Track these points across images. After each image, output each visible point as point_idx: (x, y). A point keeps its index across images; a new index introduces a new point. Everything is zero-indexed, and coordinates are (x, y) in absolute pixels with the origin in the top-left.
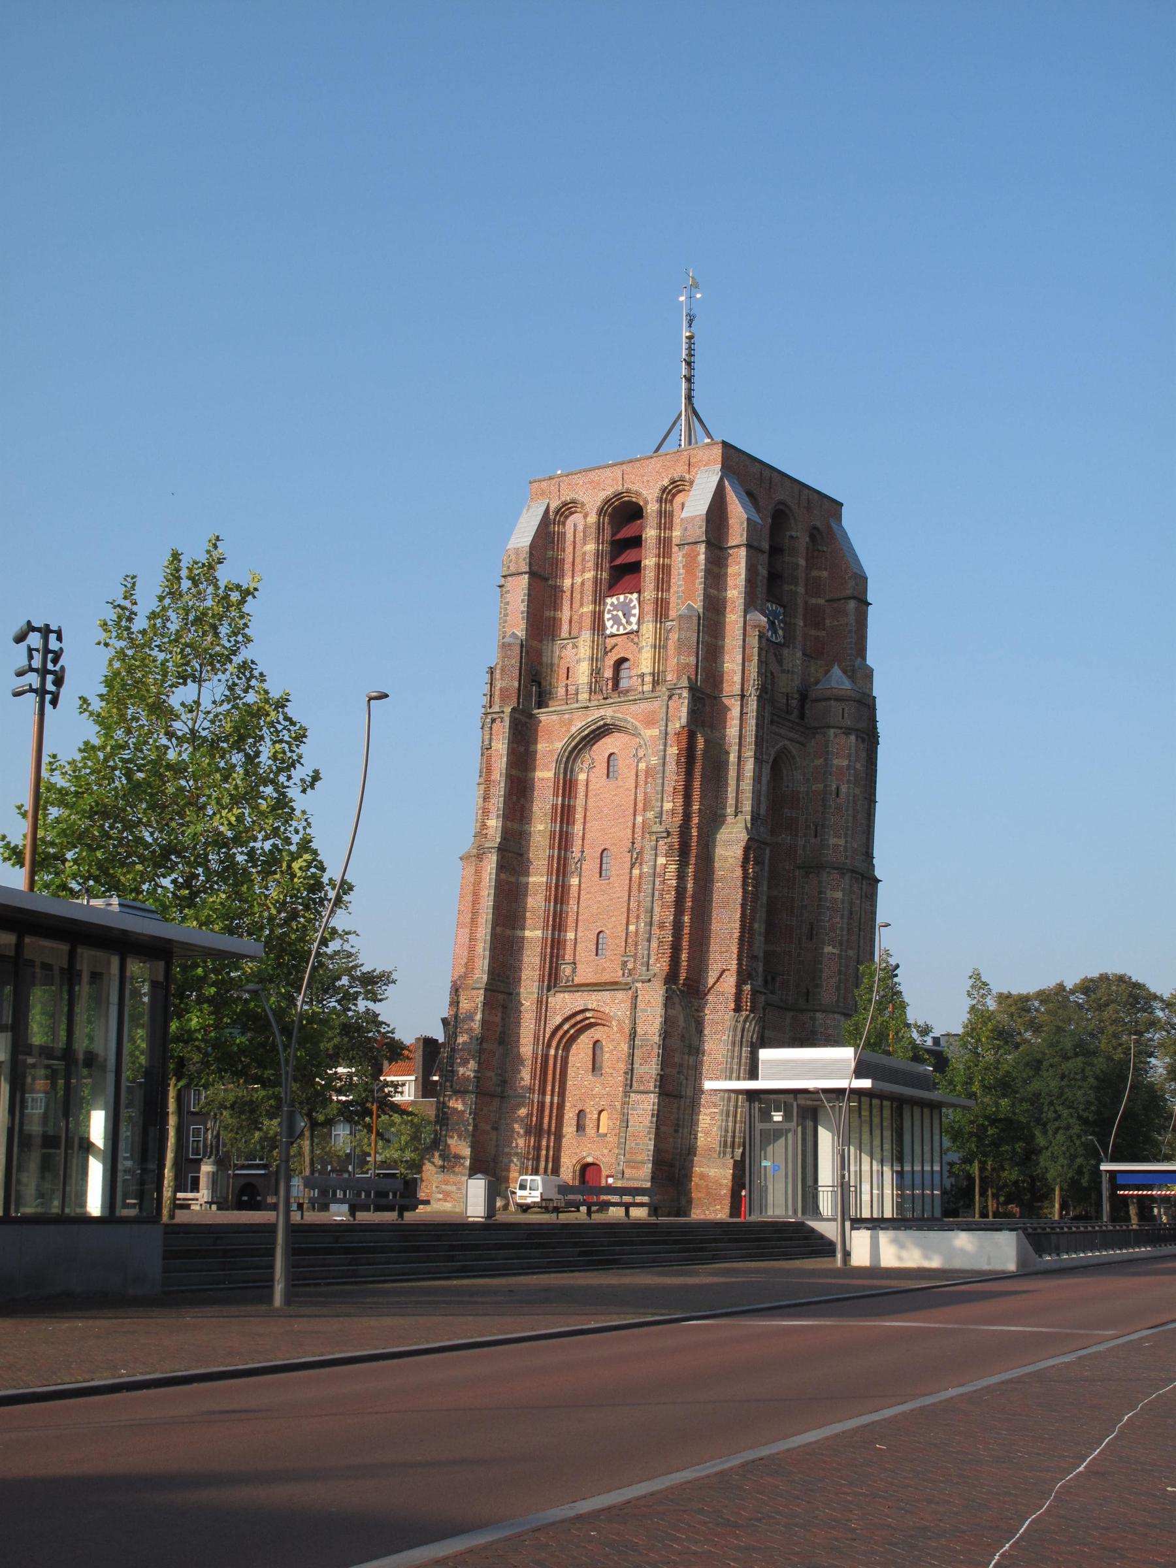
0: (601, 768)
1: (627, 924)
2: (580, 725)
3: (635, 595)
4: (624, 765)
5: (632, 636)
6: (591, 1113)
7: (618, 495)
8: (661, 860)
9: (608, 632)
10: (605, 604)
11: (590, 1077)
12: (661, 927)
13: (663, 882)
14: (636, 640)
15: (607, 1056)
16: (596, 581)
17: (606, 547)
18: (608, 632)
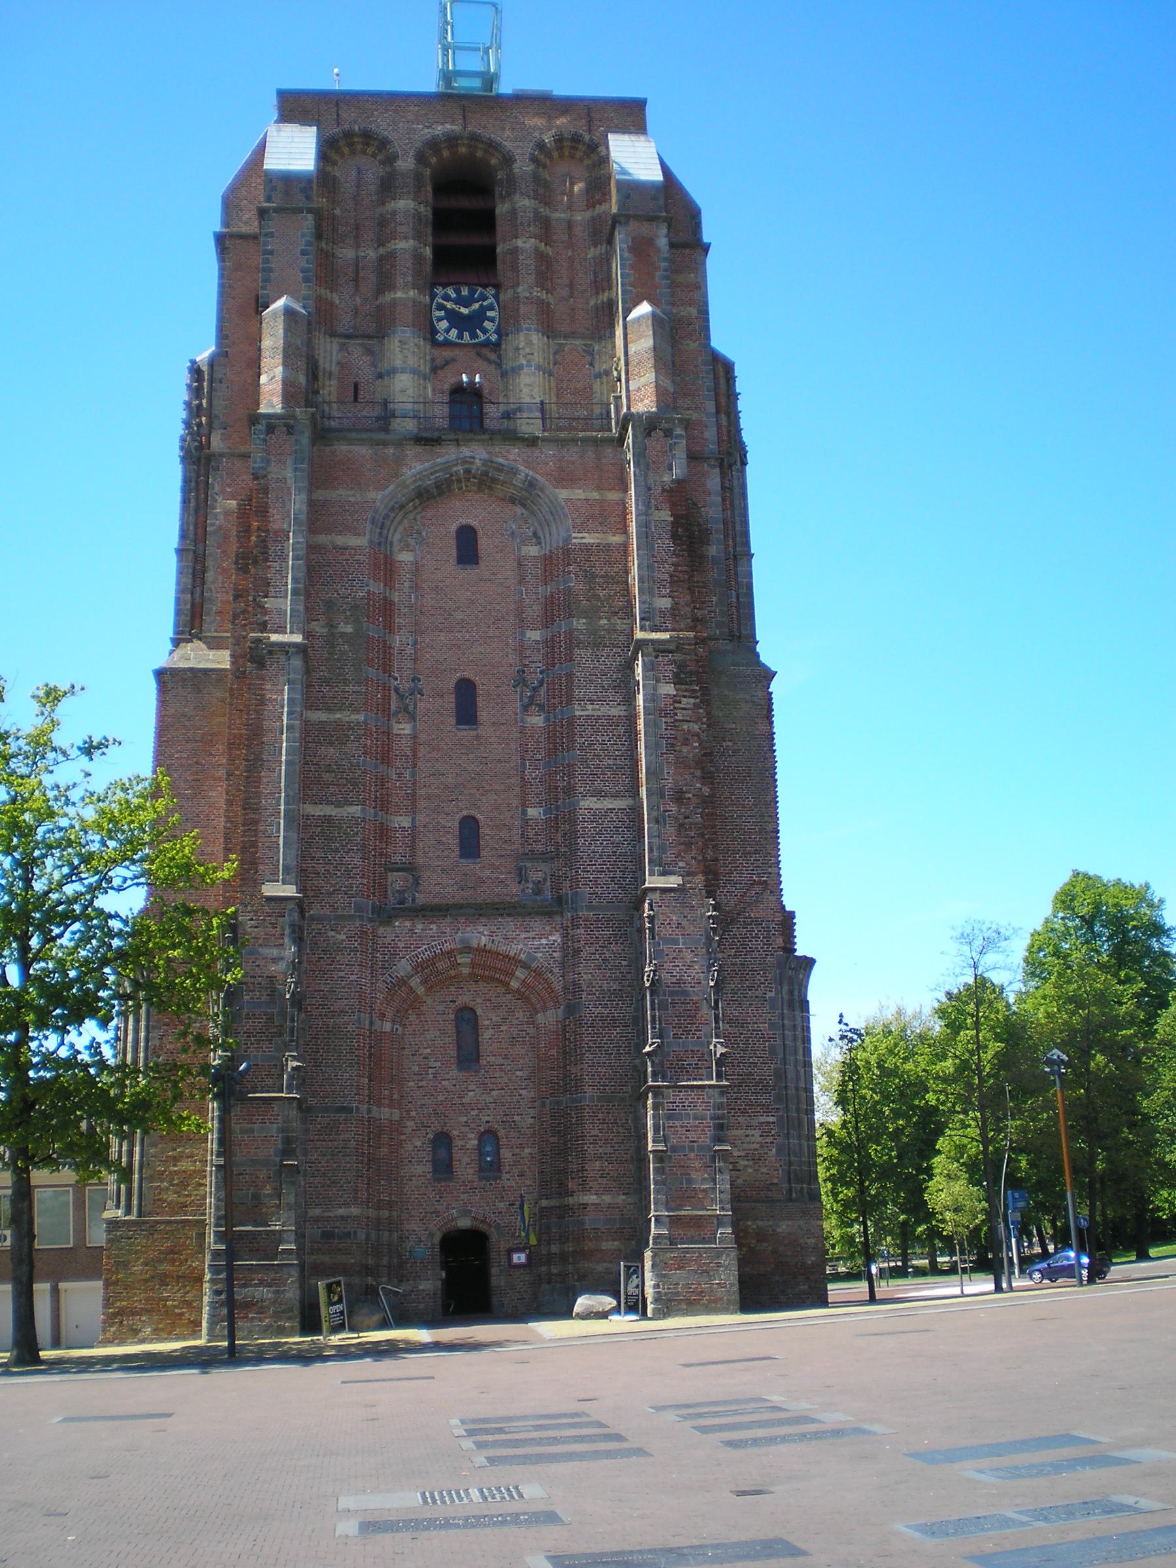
2: (419, 467)
3: (490, 291)
5: (485, 351)
6: (463, 1136)
7: (452, 140)
8: (670, 689)
9: (440, 337)
10: (433, 296)
11: (455, 1073)
13: (674, 725)
14: (493, 357)
15: (486, 1035)
16: (418, 258)
17: (426, 211)
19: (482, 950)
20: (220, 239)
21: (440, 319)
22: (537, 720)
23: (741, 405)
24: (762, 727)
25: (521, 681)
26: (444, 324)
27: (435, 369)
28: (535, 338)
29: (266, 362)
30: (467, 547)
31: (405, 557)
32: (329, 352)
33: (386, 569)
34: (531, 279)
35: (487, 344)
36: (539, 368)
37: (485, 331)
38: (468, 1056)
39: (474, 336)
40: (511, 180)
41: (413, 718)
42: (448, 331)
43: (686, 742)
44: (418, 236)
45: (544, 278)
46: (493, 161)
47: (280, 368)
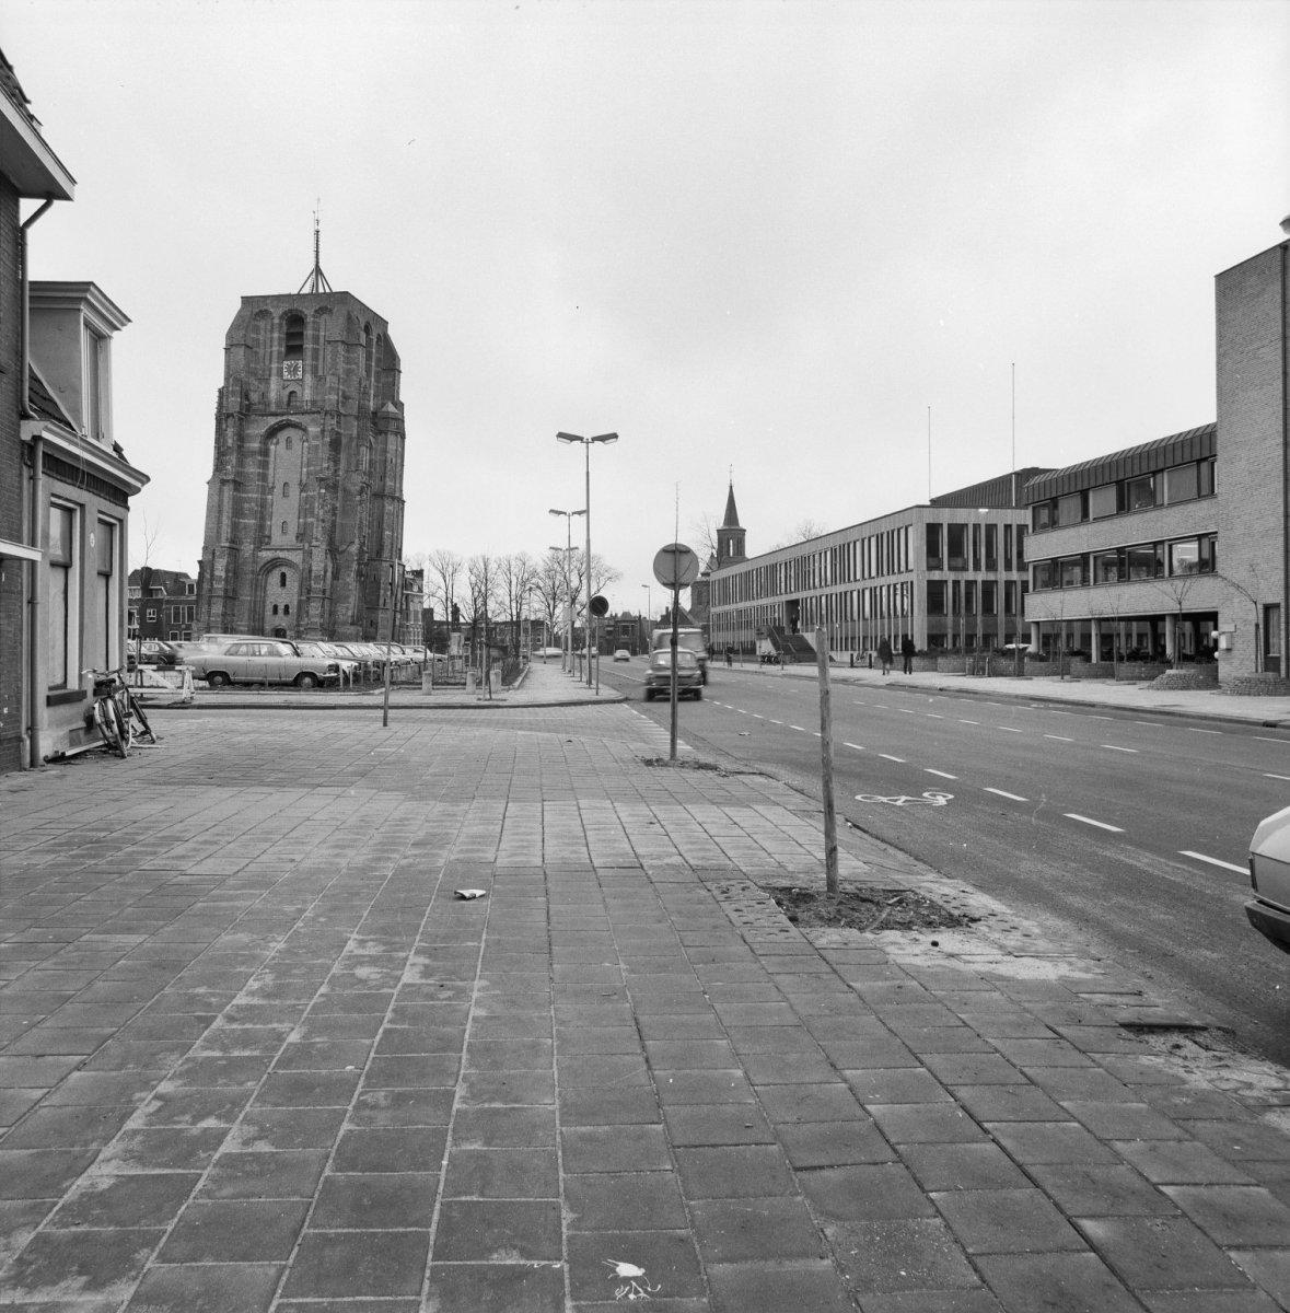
0: (283, 444)
4: (297, 445)
7: (290, 311)
12: (323, 521)
16: (279, 353)
17: (283, 336)
31: (272, 447)
33: (265, 452)
35: (298, 380)
38: (283, 584)
44: (280, 345)
45: (315, 358)
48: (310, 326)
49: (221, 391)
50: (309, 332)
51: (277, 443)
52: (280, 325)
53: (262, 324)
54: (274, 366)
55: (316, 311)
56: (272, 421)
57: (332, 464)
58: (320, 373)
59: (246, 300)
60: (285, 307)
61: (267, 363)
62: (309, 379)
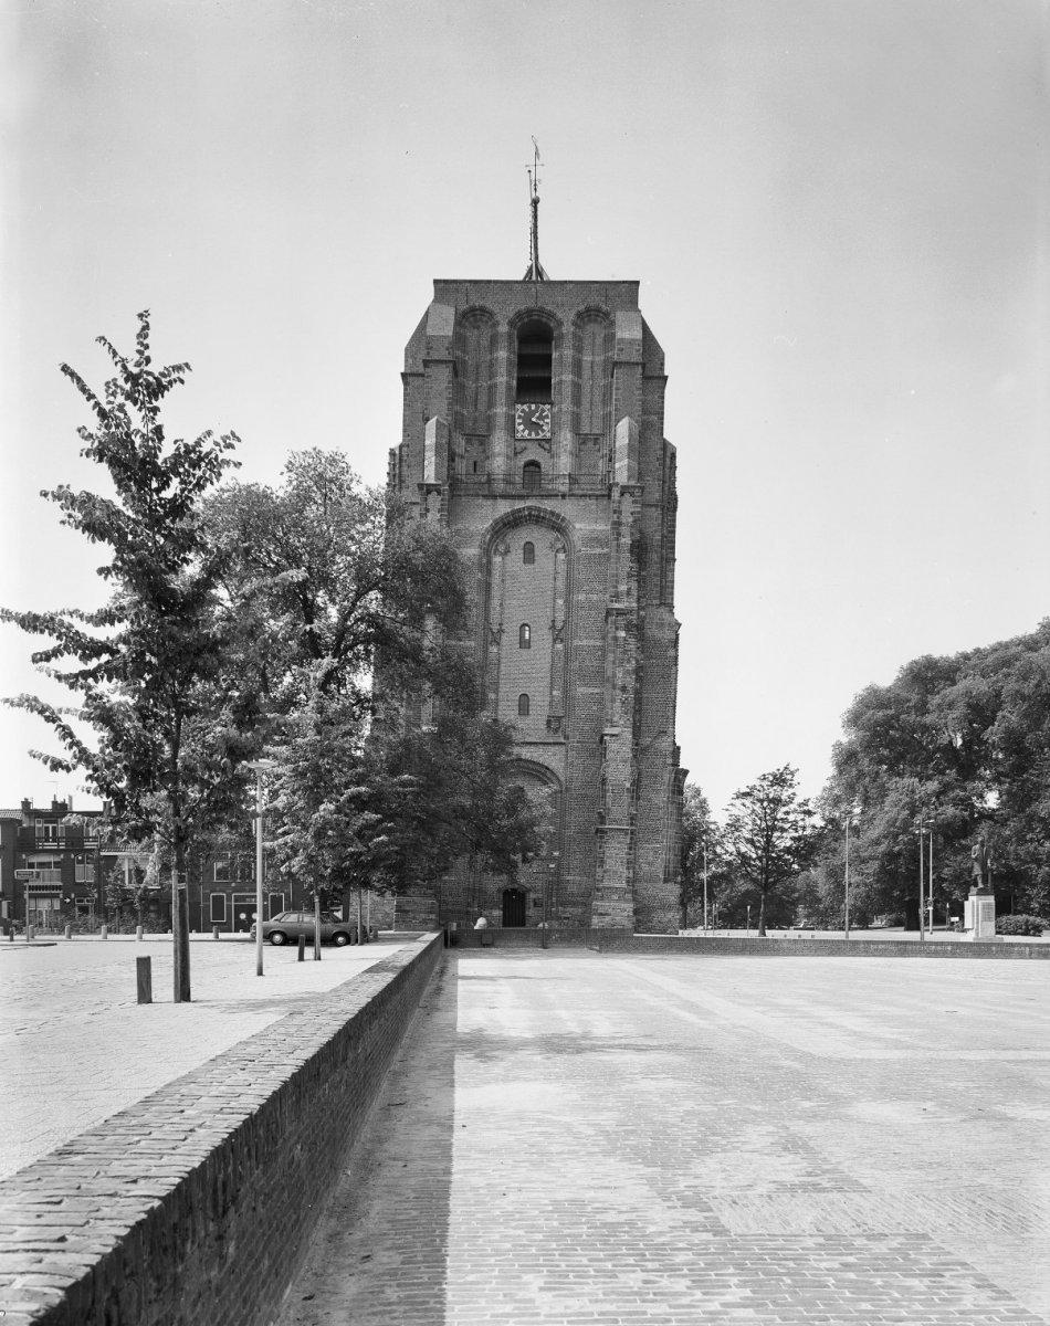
0: (517, 554)
1: (552, 688)
7: (529, 312)
9: (519, 435)
12: (624, 689)
14: (547, 446)
18: (519, 435)
19: (527, 761)
20: (404, 375)
21: (519, 424)
22: (559, 646)
23: (678, 473)
24: (671, 653)
25: (553, 627)
26: (522, 427)
27: (516, 454)
28: (569, 436)
29: (428, 454)
30: (529, 553)
31: (497, 559)
32: (460, 444)
33: (487, 568)
34: (569, 400)
36: (571, 453)
37: (543, 431)
39: (537, 434)
40: (561, 336)
41: (498, 644)
42: (523, 431)
43: (629, 661)
44: (509, 374)
45: (577, 401)
46: (552, 325)
47: (433, 458)
48: (568, 342)
49: (392, 453)
50: (562, 354)
51: (507, 552)
52: (510, 336)
53: (472, 335)
54: (500, 410)
55: (579, 315)
56: (504, 508)
57: (634, 585)
58: (585, 430)
59: (444, 288)
60: (521, 303)
61: (482, 407)
62: (566, 438)
